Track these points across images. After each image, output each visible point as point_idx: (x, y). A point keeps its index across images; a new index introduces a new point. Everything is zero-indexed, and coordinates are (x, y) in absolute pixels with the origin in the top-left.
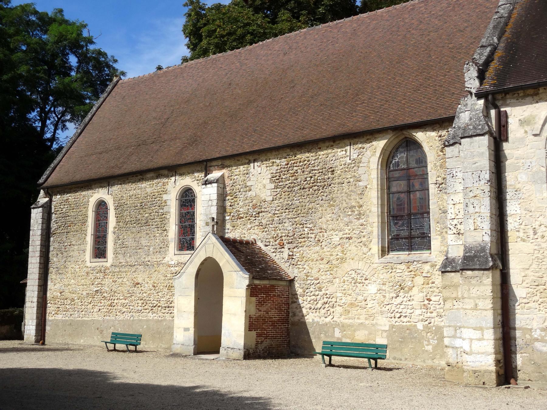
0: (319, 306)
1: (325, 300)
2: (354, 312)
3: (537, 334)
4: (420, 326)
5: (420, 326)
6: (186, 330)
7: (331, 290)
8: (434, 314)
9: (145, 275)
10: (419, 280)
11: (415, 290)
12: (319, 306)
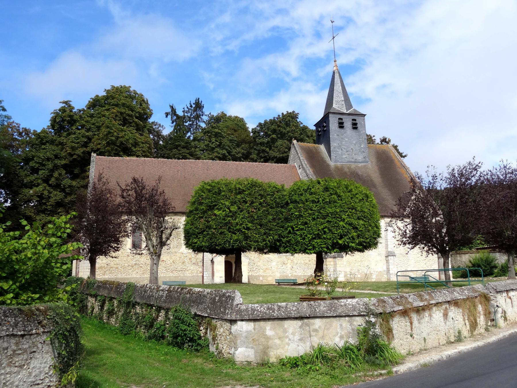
0: (254, 269)
1: (257, 267)
2: (267, 271)
3: (348, 273)
4: (290, 275)
5: (290, 275)
6: (221, 277)
7: (259, 264)
8: (294, 272)
9: (168, 257)
10: (290, 261)
11: (288, 264)
12: (254, 269)
